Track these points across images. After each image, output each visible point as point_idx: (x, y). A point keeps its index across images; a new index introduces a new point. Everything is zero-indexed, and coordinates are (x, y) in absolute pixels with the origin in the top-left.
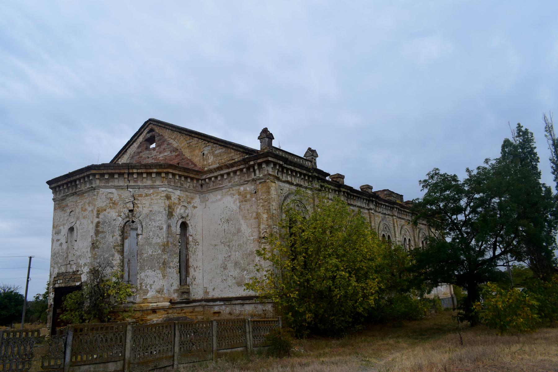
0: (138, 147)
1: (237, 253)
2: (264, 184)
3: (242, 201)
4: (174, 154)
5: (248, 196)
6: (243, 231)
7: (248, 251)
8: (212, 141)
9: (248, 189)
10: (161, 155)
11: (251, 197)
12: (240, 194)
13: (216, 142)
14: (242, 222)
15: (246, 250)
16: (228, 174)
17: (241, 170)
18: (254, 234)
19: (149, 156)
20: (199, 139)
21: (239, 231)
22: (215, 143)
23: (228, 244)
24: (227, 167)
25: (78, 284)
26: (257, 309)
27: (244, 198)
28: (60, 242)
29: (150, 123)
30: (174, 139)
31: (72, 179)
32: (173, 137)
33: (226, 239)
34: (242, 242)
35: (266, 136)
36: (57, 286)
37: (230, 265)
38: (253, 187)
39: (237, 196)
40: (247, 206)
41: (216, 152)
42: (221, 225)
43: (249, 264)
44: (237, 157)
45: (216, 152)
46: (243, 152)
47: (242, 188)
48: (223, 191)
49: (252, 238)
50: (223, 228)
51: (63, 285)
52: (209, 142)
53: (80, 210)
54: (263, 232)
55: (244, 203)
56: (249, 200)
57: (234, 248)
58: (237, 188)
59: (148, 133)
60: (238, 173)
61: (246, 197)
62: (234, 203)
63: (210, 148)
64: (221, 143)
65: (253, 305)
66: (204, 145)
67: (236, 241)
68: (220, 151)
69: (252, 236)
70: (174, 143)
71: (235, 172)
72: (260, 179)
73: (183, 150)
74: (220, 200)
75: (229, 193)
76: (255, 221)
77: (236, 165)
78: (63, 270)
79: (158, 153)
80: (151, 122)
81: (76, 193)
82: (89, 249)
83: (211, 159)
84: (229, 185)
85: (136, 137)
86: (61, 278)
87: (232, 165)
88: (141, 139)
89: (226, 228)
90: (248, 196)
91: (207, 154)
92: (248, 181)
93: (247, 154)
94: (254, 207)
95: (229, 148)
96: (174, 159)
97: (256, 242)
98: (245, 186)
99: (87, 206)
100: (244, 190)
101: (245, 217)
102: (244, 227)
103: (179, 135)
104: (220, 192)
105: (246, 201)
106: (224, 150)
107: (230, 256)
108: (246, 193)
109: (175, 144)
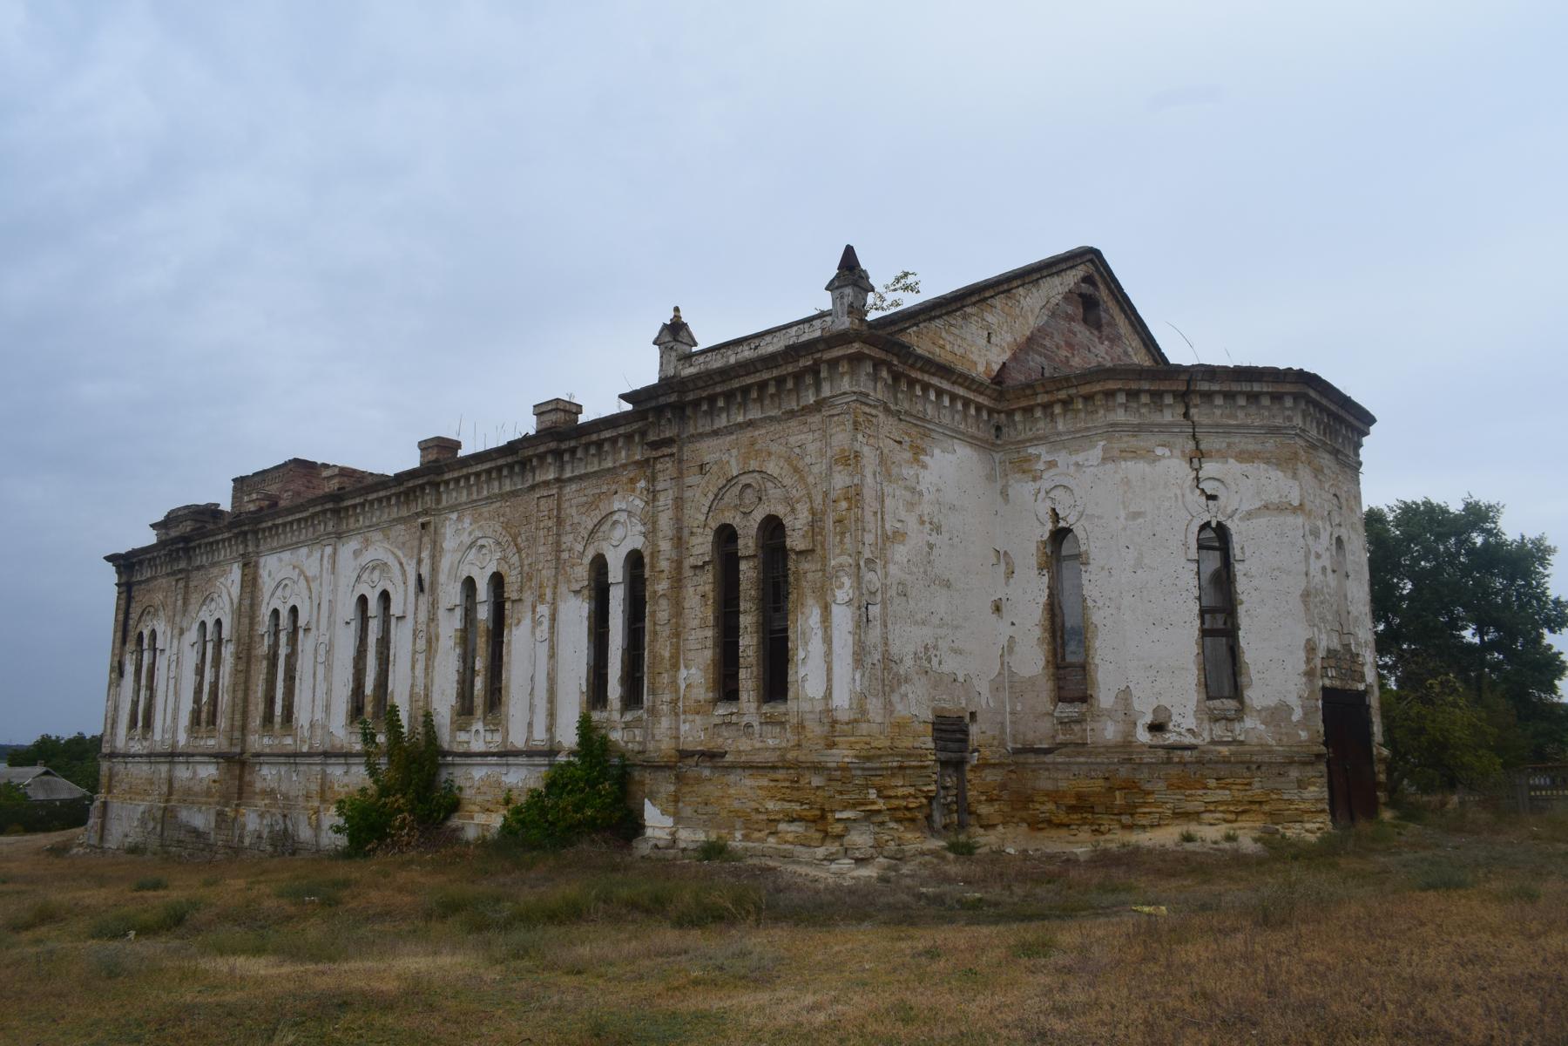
25: (1362, 687)
28: (1320, 563)
29: (1091, 261)
36: (1327, 682)
51: (1337, 683)
81: (1338, 451)
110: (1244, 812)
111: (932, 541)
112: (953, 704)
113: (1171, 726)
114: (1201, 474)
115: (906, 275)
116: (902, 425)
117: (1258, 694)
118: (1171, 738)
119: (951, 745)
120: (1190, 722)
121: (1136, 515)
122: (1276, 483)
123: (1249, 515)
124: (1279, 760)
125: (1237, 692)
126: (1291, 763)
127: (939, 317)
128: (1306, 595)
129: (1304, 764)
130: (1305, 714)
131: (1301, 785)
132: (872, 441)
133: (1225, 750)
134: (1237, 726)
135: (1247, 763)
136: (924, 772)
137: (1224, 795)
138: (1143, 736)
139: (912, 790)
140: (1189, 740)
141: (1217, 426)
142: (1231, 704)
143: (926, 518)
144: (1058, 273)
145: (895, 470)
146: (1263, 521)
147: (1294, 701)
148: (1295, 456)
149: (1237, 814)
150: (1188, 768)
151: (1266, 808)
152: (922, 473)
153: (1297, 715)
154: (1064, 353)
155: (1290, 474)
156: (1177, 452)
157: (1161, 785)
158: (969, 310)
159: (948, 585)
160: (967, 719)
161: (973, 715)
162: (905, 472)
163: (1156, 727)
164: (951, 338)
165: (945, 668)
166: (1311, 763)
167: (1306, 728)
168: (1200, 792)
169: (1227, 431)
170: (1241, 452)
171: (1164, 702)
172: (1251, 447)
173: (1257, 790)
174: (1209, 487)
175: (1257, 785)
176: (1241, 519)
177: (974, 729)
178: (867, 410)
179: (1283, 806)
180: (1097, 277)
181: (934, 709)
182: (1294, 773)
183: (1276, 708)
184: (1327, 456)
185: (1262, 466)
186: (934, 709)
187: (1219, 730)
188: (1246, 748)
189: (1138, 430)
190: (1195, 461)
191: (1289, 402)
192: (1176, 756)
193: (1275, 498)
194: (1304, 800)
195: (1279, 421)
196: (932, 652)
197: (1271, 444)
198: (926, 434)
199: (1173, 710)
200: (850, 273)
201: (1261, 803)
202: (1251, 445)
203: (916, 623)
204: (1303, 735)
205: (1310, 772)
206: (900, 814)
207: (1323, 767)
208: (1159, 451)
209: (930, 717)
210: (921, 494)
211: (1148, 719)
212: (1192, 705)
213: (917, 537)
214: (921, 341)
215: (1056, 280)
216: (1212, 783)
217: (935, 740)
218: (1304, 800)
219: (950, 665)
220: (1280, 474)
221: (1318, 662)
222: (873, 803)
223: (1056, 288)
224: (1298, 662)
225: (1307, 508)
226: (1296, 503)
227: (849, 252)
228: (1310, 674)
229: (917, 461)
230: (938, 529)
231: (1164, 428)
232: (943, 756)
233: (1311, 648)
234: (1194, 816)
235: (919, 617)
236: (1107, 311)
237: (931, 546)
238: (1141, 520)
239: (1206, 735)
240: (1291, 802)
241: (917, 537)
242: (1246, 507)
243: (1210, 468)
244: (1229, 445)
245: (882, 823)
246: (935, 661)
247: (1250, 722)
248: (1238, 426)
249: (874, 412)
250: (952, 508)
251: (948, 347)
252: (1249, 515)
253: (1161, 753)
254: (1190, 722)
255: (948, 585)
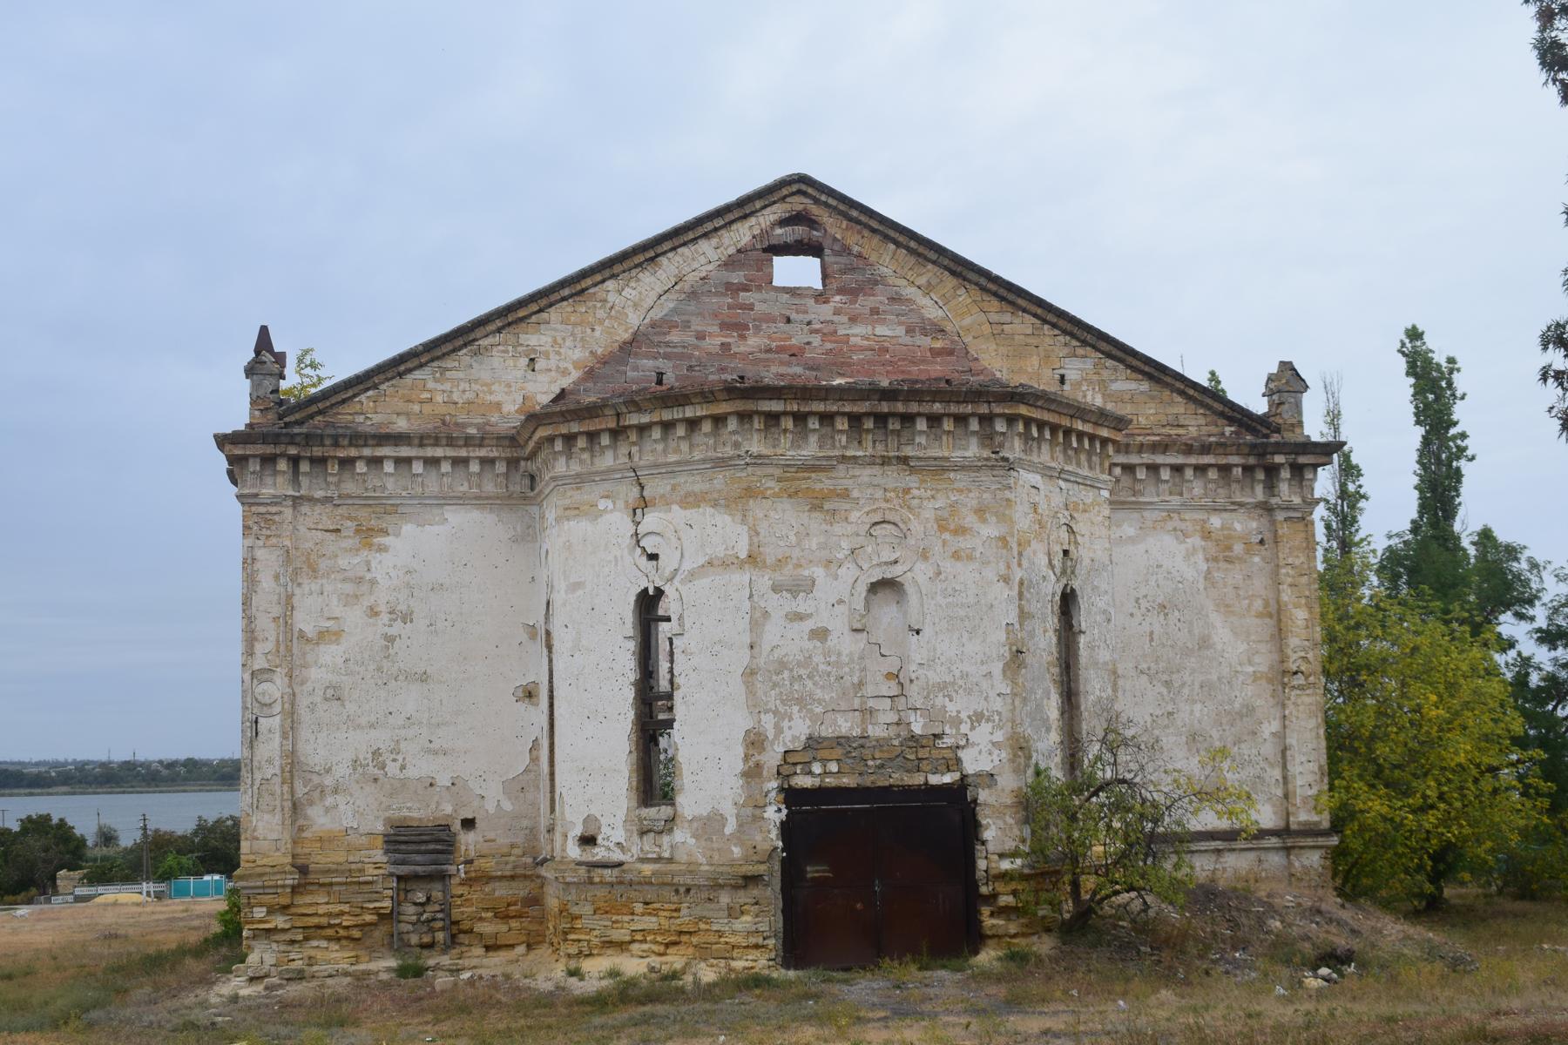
0: (729, 264)
1: (1198, 706)
2: (1300, 526)
3: (1215, 559)
4: (926, 342)
5: (1238, 548)
6: (1219, 647)
7: (1237, 705)
8: (1103, 345)
9: (1238, 527)
10: (859, 330)
11: (1247, 552)
12: (1207, 535)
13: (1115, 352)
14: (1216, 618)
15: (1231, 702)
16: (1178, 469)
17: (1225, 469)
18: (1257, 659)
19: (793, 316)
20: (1045, 321)
21: (1205, 643)
22: (1109, 356)
23: (1165, 677)
24: (1188, 450)
26: (1265, 865)
27: (1222, 551)
29: (799, 192)
30: (927, 289)
31: (900, 407)
32: (922, 281)
33: (1157, 662)
34: (1214, 677)
35: (1287, 383)
37: (1172, 739)
38: (1254, 525)
39: (1196, 541)
40: (1236, 575)
41: (1116, 386)
42: (1138, 618)
43: (1238, 741)
44: (1195, 425)
45: (1116, 386)
46: (1222, 415)
47: (1216, 521)
48: (1146, 514)
49: (1251, 669)
50: (1146, 627)
52: (1084, 343)
53: (932, 526)
54: (1294, 656)
55: (1223, 565)
56: (1240, 560)
57: (1186, 691)
58: (1201, 516)
59: (783, 223)
60: (1213, 474)
61: (1229, 548)
62: (1187, 557)
63: (1088, 365)
64: (1135, 363)
65: (1252, 856)
66: (1066, 351)
67: (1193, 671)
68: (1133, 386)
69: (1250, 663)
70: (925, 301)
71: (1201, 469)
72: (1289, 508)
73: (968, 339)
74: (1132, 540)
75: (1170, 525)
76: (1258, 621)
77: (1221, 450)
78: (846, 725)
79: (845, 319)
80: (801, 184)
82: (997, 668)
83: (1149, 412)
84: (1176, 500)
85: (719, 222)
86: (838, 752)
87: (1206, 449)
88: (742, 234)
89: (1158, 630)
90: (1238, 548)
91: (1079, 384)
92: (1241, 505)
93: (1231, 421)
94: (1260, 584)
95: (1167, 385)
96: (923, 361)
97: (1263, 682)
98: (1226, 515)
99: (970, 520)
100: (1222, 529)
101: (1225, 608)
102: (1221, 634)
103: (951, 282)
104: (1136, 515)
105: (1228, 560)
106: (1145, 386)
107: (1170, 714)
108: (1229, 537)
109: (931, 311)
110: (675, 943)
111: (392, 631)
112: (418, 811)
113: (599, 840)
114: (641, 530)
115: (306, 352)
116: (340, 511)
117: (691, 801)
118: (599, 853)
119: (418, 858)
120: (619, 835)
121: (577, 586)
122: (723, 531)
123: (692, 575)
124: (702, 882)
125: (667, 797)
126: (722, 887)
127: (421, 366)
128: (750, 673)
129: (736, 887)
130: (740, 826)
131: (733, 913)
132: (274, 540)
133: (647, 869)
134: (666, 839)
135: (675, 887)
136: (366, 888)
137: (650, 922)
138: (574, 851)
139: (346, 908)
140: (617, 856)
141: (657, 466)
142: (665, 811)
143: (383, 608)
144: (706, 235)
145: (323, 565)
146: (705, 582)
147: (729, 811)
148: (750, 493)
149: (667, 945)
150: (614, 886)
151: (695, 940)
152: (376, 558)
153: (729, 829)
154: (713, 343)
155: (739, 517)
156: (620, 504)
157: (587, 909)
158: (484, 342)
159: (424, 678)
160: (457, 826)
161: (469, 824)
162: (342, 562)
163: (588, 841)
164: (447, 386)
165: (411, 772)
166: (745, 887)
167: (741, 843)
168: (626, 918)
169: (670, 470)
170: (688, 495)
171: (595, 811)
172: (697, 488)
173: (685, 919)
174: (650, 544)
175: (684, 912)
176: (682, 582)
177: (468, 842)
178: (262, 509)
179: (713, 939)
180: (815, 210)
181: (388, 821)
182: (725, 898)
183: (709, 818)
184: (868, 471)
185: (709, 510)
186: (388, 821)
187: (648, 844)
188: (673, 867)
189: (580, 480)
190: (639, 512)
191: (732, 424)
192: (597, 874)
193: (720, 552)
194: (734, 933)
195: (729, 451)
196: (387, 757)
197: (720, 479)
198: (393, 510)
199: (603, 821)
200: (265, 360)
201: (690, 933)
202: (697, 484)
203: (359, 726)
204: (737, 851)
205: (743, 897)
206: (330, 932)
207: (771, 893)
208: (602, 504)
209: (380, 827)
210: (373, 582)
211: (578, 831)
212: (621, 815)
213: (359, 630)
214: (371, 412)
215: (705, 246)
216: (639, 908)
217: (387, 852)
218: (734, 933)
219: (420, 768)
220: (728, 519)
221: (771, 758)
222: (261, 922)
223: (705, 256)
224: (735, 760)
225: (770, 554)
226: (743, 555)
227: (264, 332)
228: (752, 773)
229: (371, 545)
230: (407, 618)
231: (606, 474)
232: (404, 870)
233: (755, 742)
234: (621, 946)
235: (363, 721)
236: (846, 250)
237: (390, 639)
238: (580, 592)
239: (635, 850)
240: (720, 933)
241: (359, 630)
242: (687, 566)
243: (651, 520)
244: (674, 488)
245: (293, 942)
246: (392, 769)
247: (680, 835)
248: (678, 463)
249: (274, 509)
250: (436, 588)
251: (439, 398)
252: (692, 575)
253: (582, 871)
254: (619, 835)
255: (424, 678)
